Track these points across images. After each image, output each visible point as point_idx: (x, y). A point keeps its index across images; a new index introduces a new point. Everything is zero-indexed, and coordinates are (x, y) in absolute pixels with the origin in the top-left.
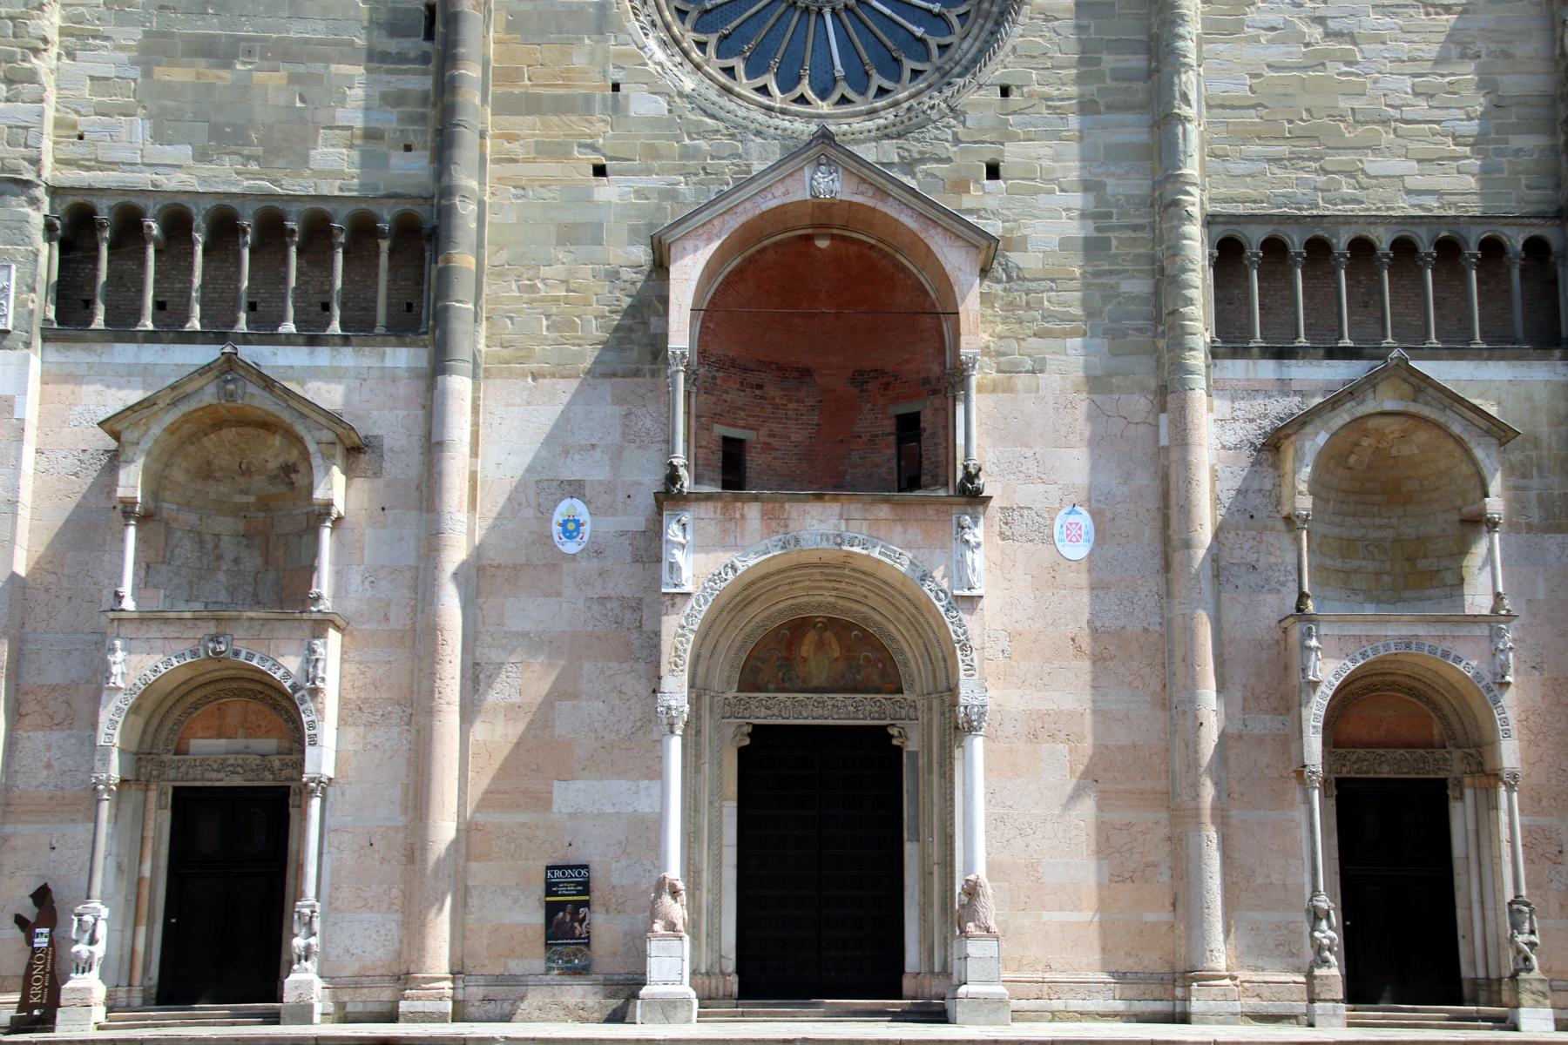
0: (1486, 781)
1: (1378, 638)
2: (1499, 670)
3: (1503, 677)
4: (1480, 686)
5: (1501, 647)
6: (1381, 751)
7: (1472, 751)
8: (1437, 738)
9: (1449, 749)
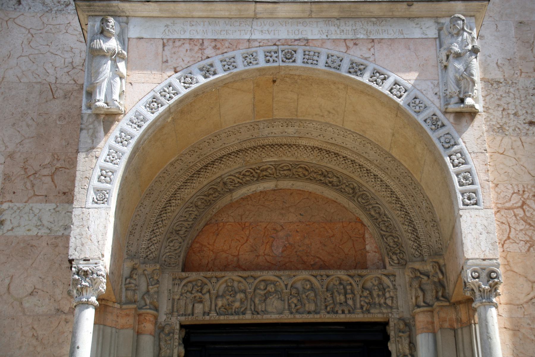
0: (451, 314)
1: (235, 44)
2: (453, 88)
3: (462, 101)
4: (420, 119)
5: (456, 48)
6: (269, 275)
7: (428, 267)
8: (372, 256)
9: (390, 269)
